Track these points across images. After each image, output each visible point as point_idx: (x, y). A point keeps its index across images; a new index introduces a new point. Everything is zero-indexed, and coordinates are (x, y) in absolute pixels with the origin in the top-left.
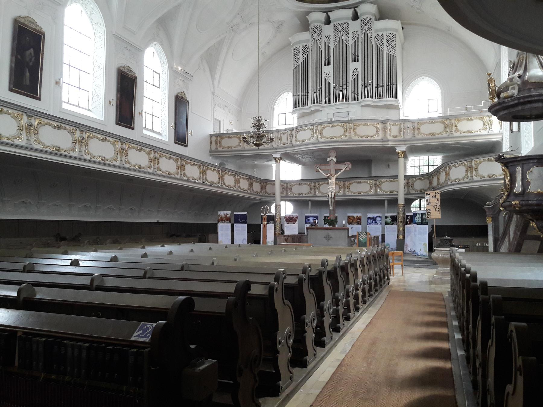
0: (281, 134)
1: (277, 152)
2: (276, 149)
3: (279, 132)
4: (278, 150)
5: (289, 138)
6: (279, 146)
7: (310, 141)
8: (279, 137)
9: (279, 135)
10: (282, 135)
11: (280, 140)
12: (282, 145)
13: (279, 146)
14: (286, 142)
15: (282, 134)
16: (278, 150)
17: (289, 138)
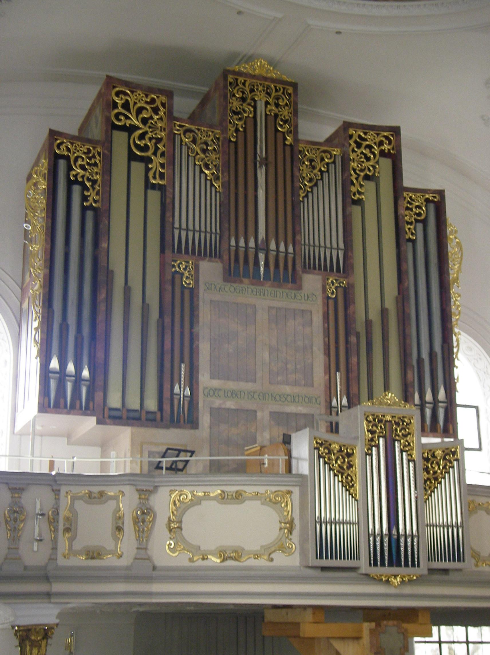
0: (73, 499)
1: (48, 595)
2: (47, 579)
3: (64, 490)
4: (57, 587)
5: (128, 526)
6: (61, 561)
7: (272, 560)
8: (64, 513)
9: (65, 501)
10: (79, 505)
11: (67, 530)
12: (82, 560)
13: (61, 561)
14: (109, 545)
15: (81, 498)
16: (57, 587)
17: (128, 526)
